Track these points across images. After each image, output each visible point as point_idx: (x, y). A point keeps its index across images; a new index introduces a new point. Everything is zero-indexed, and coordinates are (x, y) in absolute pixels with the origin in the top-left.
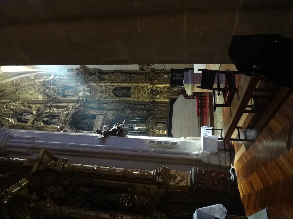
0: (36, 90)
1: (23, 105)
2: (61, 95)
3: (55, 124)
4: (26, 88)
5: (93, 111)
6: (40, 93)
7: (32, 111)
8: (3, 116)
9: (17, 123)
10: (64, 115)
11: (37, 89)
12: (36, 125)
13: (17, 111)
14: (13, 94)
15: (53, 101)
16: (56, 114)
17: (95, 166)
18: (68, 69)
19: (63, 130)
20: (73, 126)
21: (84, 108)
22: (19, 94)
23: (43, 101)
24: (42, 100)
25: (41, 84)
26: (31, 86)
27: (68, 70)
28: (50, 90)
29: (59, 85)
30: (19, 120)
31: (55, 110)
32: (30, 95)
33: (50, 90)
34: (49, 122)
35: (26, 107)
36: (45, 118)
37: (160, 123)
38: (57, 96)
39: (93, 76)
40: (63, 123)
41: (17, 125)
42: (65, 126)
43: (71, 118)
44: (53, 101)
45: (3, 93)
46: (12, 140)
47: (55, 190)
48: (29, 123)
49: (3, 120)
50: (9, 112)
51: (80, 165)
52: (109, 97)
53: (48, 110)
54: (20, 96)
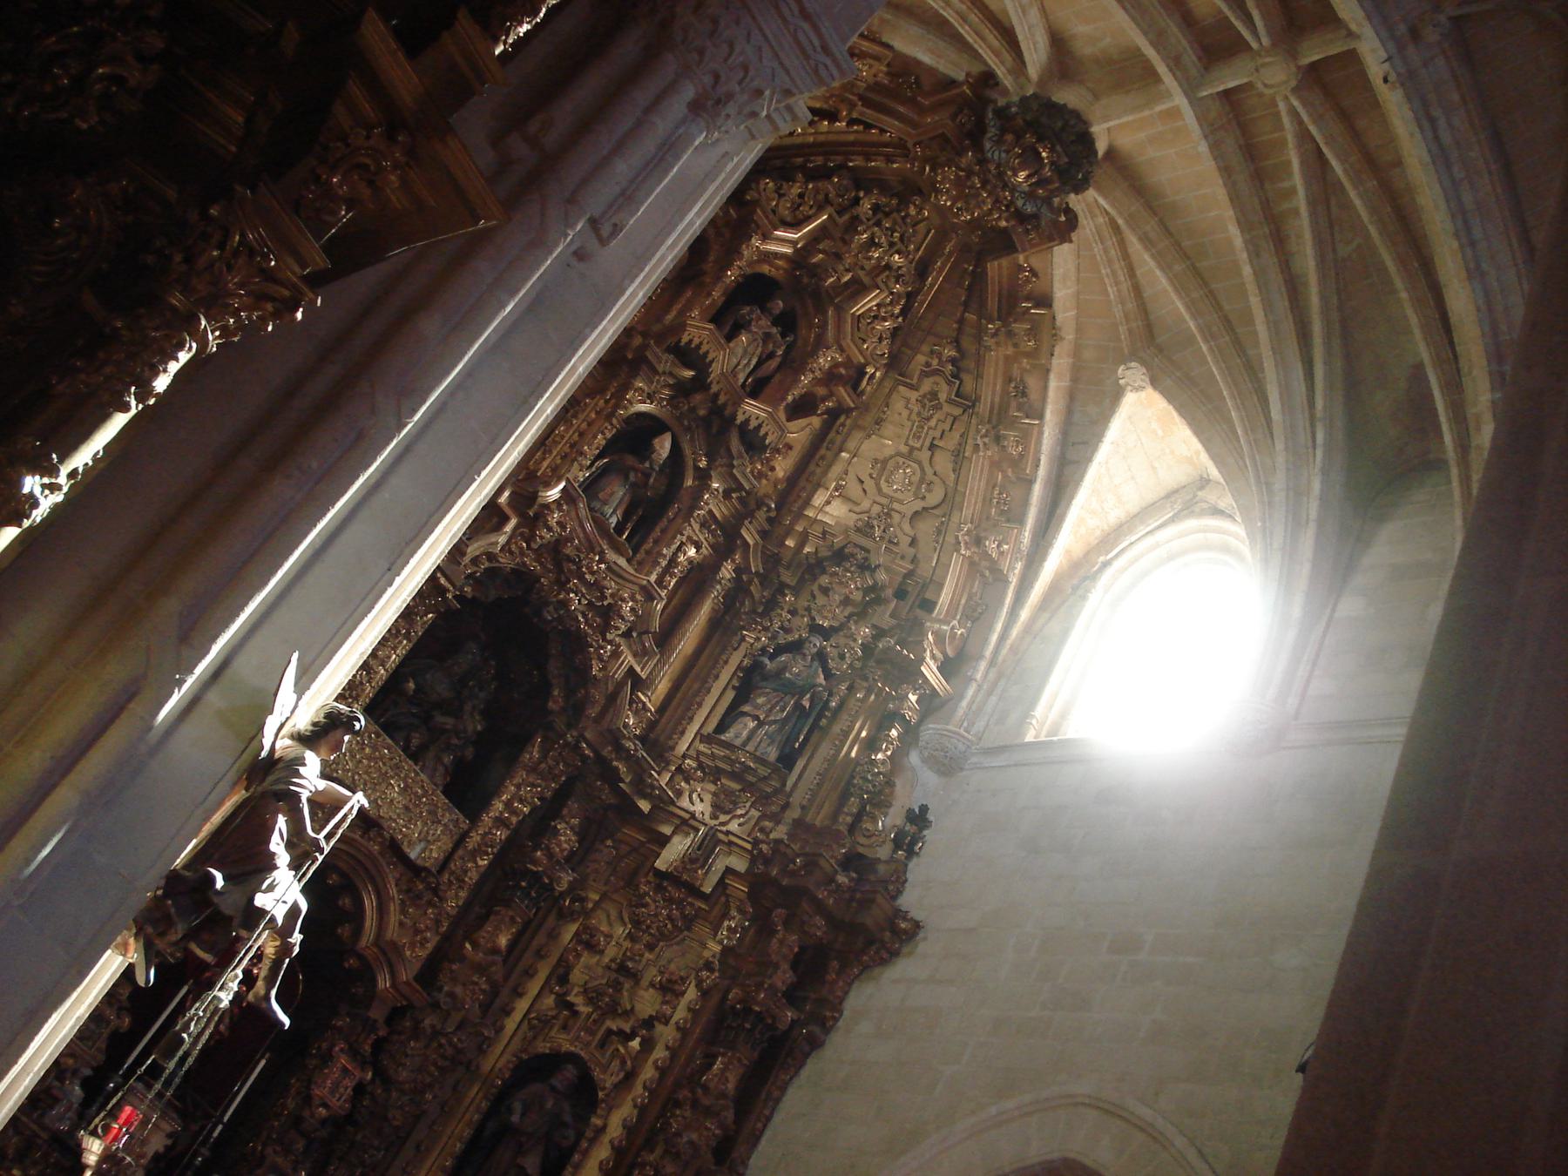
0: (896, 517)
1: (841, 376)
2: (772, 657)
3: (591, 487)
4: (943, 462)
5: (514, 812)
6: (866, 529)
7: (774, 403)
8: (840, 213)
9: (751, 264)
10: (611, 586)
11: (903, 530)
12: (665, 362)
13: (825, 313)
14: (953, 361)
15: (764, 579)
16: (656, 542)
17: (53, 488)
18: (930, 817)
19: (508, 511)
20: (493, 594)
21: (584, 758)
22: (934, 395)
23: (800, 515)
24: (810, 513)
25: (925, 570)
26: (943, 501)
27: (924, 809)
28: (849, 610)
29: (851, 688)
30: (756, 289)
31: (692, 552)
32: (885, 462)
33: (849, 610)
34: (630, 460)
35: (817, 382)
36: (676, 448)
38: (776, 626)
39: (783, 977)
40: (556, 547)
41: (731, 253)
43: (560, 619)
44: (764, 579)
45: (992, 304)
46: (688, 92)
47: (102, 78)
48: (698, 331)
49: (821, 197)
50: (848, 261)
51: (161, 383)
52: (549, 1001)
53: (713, 504)
54: (914, 395)
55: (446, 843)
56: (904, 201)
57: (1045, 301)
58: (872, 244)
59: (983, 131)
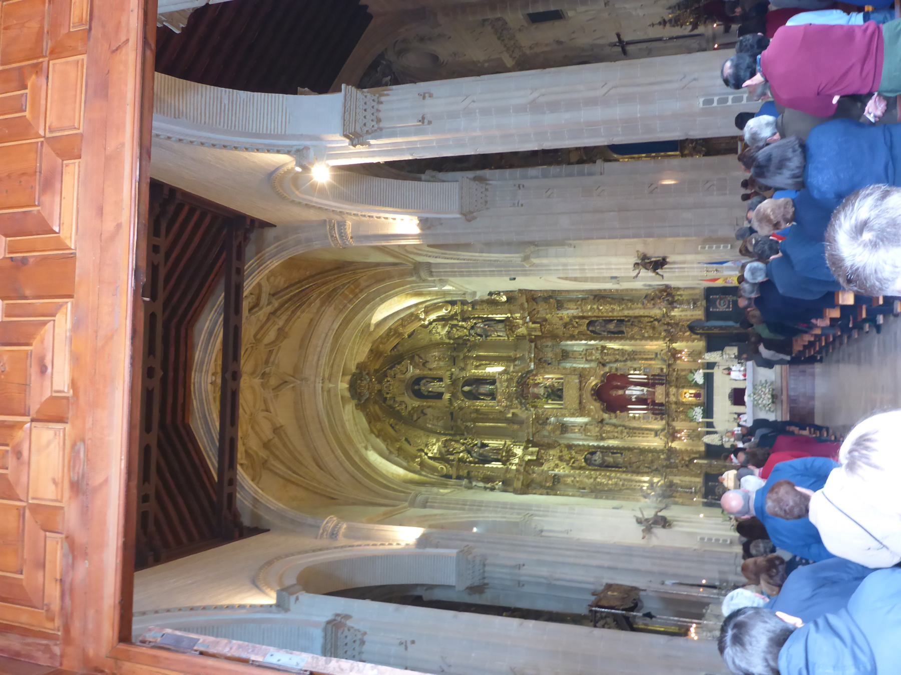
33: (458, 328)
42: (511, 405)
55: (570, 376)
57: (371, 351)
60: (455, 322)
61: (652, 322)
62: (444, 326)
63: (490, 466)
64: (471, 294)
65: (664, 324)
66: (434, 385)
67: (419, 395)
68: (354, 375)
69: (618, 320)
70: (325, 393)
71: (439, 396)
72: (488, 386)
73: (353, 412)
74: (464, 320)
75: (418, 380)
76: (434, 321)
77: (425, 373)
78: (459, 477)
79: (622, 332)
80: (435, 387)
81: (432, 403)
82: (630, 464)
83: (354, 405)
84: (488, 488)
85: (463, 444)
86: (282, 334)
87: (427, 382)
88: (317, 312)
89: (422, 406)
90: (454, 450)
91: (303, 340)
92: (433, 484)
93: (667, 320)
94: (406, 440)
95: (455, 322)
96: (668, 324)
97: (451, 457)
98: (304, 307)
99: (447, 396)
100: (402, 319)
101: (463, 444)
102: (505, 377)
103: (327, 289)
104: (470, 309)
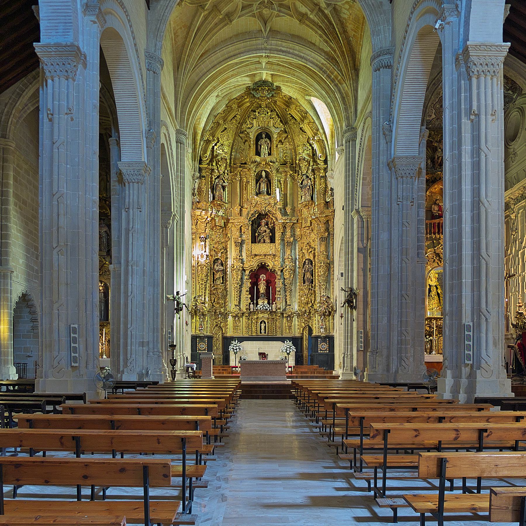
37: (265, 327)
56: (261, 107)
57: (291, 98)
58: (263, 117)
59: (254, 95)
60: (311, 164)
61: (311, 302)
62: (309, 155)
63: (210, 193)
64: (332, 174)
65: (310, 310)
66: (266, 149)
67: (259, 138)
68: (272, 84)
69: (312, 280)
70: (258, 59)
71: (258, 153)
72: (265, 190)
73: (244, 84)
74: (313, 170)
75: (269, 137)
76: (313, 148)
77: (275, 142)
78: (200, 170)
79: (304, 283)
80: (264, 150)
81: (253, 148)
82: (216, 288)
83: (249, 85)
84: (194, 191)
85: (224, 172)
86: (302, 17)
87: (268, 144)
88: (320, 49)
89: (250, 141)
90: (220, 165)
91: (298, 37)
92: (194, 150)
93: (313, 312)
94: (226, 129)
95: (311, 164)
96: (310, 313)
97: (214, 164)
98: (324, 36)
99: (258, 159)
100: (314, 122)
101: (224, 172)
102: (272, 202)
103: (338, 57)
104: (321, 174)
